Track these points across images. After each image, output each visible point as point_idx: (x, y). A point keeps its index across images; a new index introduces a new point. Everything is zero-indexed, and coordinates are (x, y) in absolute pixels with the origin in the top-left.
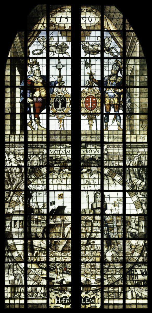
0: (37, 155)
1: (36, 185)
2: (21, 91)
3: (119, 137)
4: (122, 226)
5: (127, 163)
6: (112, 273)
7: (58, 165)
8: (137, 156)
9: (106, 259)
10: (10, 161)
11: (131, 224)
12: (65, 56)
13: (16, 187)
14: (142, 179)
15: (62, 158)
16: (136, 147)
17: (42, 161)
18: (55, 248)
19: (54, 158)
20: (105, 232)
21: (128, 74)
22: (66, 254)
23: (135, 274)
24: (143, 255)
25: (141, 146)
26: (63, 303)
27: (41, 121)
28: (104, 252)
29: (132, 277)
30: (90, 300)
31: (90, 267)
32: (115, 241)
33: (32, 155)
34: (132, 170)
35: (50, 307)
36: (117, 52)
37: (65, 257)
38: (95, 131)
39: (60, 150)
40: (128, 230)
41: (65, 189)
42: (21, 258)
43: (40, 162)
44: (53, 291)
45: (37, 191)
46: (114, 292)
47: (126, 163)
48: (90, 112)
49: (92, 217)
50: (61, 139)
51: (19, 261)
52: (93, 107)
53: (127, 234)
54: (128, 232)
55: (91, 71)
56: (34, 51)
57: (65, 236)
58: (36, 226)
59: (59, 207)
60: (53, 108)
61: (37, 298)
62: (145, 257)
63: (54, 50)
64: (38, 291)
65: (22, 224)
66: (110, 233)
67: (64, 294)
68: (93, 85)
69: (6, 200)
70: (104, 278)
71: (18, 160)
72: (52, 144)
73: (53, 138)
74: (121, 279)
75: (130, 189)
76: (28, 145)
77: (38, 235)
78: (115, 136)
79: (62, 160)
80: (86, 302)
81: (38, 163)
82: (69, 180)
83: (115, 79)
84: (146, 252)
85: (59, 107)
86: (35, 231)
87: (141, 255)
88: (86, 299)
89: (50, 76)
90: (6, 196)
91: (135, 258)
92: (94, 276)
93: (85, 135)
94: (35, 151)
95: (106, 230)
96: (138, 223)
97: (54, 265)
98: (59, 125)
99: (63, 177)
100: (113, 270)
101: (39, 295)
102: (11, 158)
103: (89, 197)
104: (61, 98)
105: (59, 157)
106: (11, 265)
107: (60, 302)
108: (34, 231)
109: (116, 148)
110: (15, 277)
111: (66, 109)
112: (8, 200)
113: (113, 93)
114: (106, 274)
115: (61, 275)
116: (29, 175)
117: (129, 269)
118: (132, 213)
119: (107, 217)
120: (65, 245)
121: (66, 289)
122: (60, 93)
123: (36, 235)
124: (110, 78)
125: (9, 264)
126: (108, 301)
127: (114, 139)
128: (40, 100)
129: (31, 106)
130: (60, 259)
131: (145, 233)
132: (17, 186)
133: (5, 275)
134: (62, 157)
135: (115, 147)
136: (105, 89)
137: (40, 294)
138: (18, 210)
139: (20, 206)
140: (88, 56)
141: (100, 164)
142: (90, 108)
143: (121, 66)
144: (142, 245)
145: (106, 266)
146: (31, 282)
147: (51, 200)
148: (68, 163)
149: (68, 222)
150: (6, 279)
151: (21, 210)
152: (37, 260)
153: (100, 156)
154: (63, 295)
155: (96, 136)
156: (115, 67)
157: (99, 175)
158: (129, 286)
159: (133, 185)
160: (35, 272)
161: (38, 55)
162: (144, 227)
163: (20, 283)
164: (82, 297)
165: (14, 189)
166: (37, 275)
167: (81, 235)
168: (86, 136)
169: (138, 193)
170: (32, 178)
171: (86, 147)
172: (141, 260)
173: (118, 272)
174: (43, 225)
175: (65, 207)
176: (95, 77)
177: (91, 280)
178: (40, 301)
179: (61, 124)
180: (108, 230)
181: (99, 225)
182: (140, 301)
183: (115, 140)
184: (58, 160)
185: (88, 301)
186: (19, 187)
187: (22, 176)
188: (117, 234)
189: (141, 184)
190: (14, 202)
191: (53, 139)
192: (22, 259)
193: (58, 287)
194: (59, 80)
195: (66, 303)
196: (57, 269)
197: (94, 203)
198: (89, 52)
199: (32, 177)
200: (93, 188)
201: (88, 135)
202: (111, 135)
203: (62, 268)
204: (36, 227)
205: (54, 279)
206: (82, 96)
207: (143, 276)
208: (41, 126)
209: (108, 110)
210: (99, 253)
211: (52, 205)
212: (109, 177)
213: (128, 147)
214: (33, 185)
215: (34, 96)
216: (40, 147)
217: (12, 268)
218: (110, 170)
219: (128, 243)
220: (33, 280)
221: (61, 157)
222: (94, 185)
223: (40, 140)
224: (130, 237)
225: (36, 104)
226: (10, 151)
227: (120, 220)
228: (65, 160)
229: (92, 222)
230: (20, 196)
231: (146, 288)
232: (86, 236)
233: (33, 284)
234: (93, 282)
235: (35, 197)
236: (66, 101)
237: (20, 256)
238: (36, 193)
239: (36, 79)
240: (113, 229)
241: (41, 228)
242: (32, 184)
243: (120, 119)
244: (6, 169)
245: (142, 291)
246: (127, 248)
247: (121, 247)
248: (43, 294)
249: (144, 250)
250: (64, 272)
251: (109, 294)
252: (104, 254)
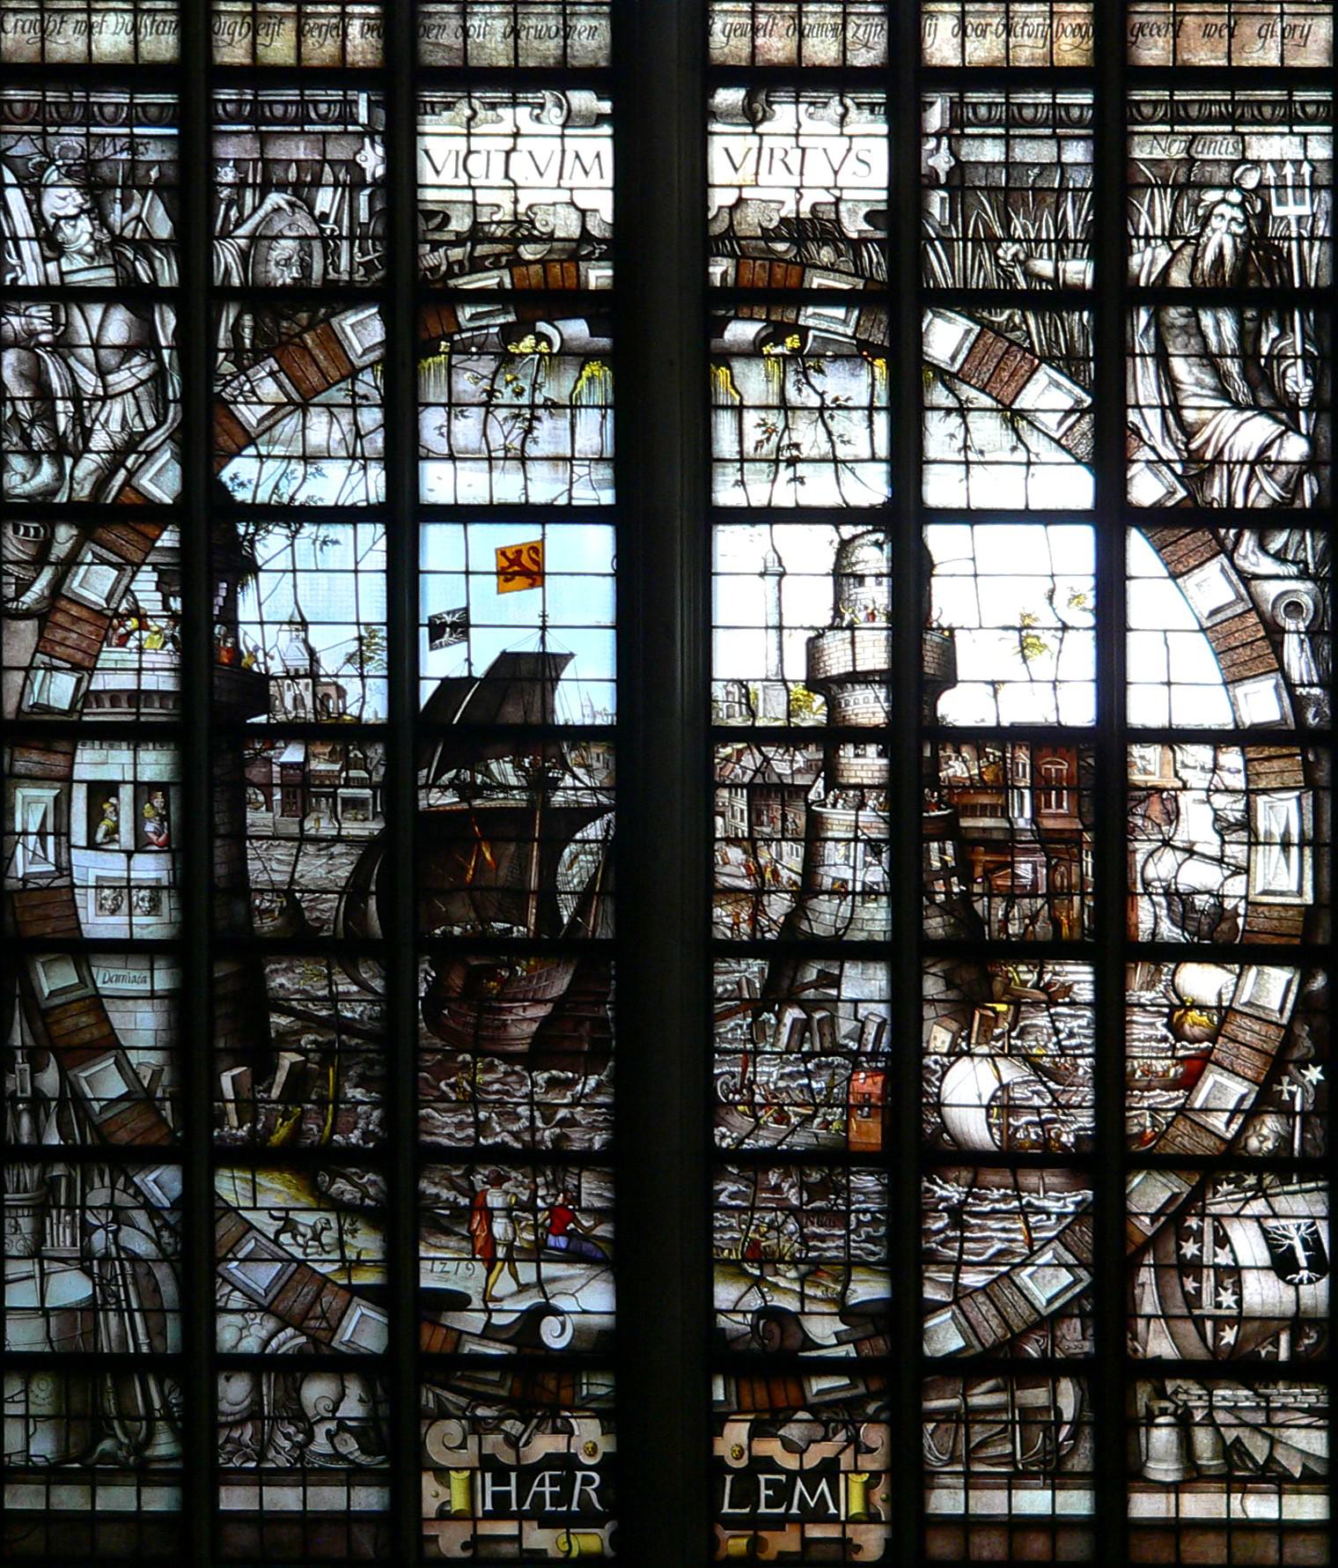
0: (302, 192)
1: (298, 468)
3: (1066, 22)
4: (1087, 837)
5: (1146, 261)
6: (1000, 1253)
7: (500, 284)
8: (1235, 196)
9: (944, 1127)
10: (51, 242)
11: (1173, 816)
13: (102, 483)
14: (1283, 409)
15: (532, 222)
16: (1221, 120)
17: (345, 245)
18: (477, 1026)
19: (460, 223)
20: (939, 886)
22: (570, 1084)
23: (1216, 1267)
24: (1286, 1097)
25: (1267, 111)
26: (548, 1508)
28: (929, 1061)
29: (1190, 1285)
30: (800, 1485)
31: (795, 1202)
32: (1022, 968)
33: (254, 186)
34: (1184, 328)
35: (430, 1550)
37: (562, 1113)
39: (514, 149)
40: (1151, 873)
41: (562, 501)
42: (158, 1112)
43: (331, 254)
44: (451, 1408)
45: (294, 515)
46: (1013, 1422)
47: (1135, 260)
49: (813, 753)
51: (138, 1141)
53: (1143, 903)
54: (1146, 884)
57: (566, 920)
58: (295, 830)
59: (507, 660)
61: (305, 1472)
62: (1302, 1112)
64: (310, 1412)
65: (164, 818)
66: (982, 896)
67: (555, 1431)
69: (16, 599)
70: (930, 1293)
71: (128, 233)
72: (437, 96)
73: (450, 38)
74: (1081, 1308)
75: (1171, 493)
76: (223, 95)
77: (312, 909)
78: (1028, 16)
79: (532, 239)
80: (762, 1510)
81: (310, 266)
82: (595, 414)
84: (1314, 1074)
86: (286, 878)
87: (1266, 1100)
88: (762, 1478)
90: (17, 563)
91: (1218, 1122)
92: (836, 1281)
94: (279, 151)
95: (942, 860)
96: (1241, 805)
97: (465, 1184)
99: (535, 387)
100: (1004, 1230)
101: (321, 1444)
102: (58, 218)
103: (785, 579)
105: (508, 208)
106: (63, 1182)
107: (520, 1503)
108: (276, 877)
109: (1033, 123)
110: (101, 1283)
112: (29, 598)
114: (944, 1263)
115: (527, 1272)
116: (227, 368)
117: (1154, 1217)
118: (1186, 719)
119: (958, 752)
120: (559, 1002)
121: (565, 1394)
123: (293, 910)
125: (43, 1173)
126: (962, 1494)
127: (1012, 40)
130: (515, 1128)
131: (1308, 898)
132: (113, 473)
133: (13, 1269)
134: (530, 207)
135: (1028, 113)
137: (330, 1436)
138: (126, 682)
139: (141, 650)
141: (881, 275)
144: (1281, 1010)
145: (940, 1192)
146: (247, 1327)
147: (437, 598)
148: (583, 265)
149: (588, 800)
150: (20, 1295)
151: (149, 682)
152: (297, 1132)
153: (883, 207)
154: (545, 1444)
157: (874, 379)
158: (1160, 1369)
159: (1193, 458)
160: (285, 1238)
162: (1301, 846)
163: (142, 1338)
164: (722, 1457)
165: (87, 491)
166: (302, 1263)
167: (717, 911)
169: (1239, 537)
170: (261, 403)
171: (752, 116)
172: (1269, 1145)
173: (1056, 1244)
174: (352, 828)
175: (564, 659)
177: (803, 1313)
178: (330, 1498)
180: (964, 869)
181: (872, 820)
182: (1260, 1507)
183: (1028, 52)
184: (493, 240)
185: (782, 1493)
186: (134, 482)
187: (158, 378)
188: (1040, 902)
189: (1273, 454)
190: (85, 614)
191: (450, 48)
192: (165, 1120)
193: (494, 1376)
195: (575, 1508)
196: (489, 1215)
197: (831, 627)
199: (253, 391)
200: (820, 489)
203: (531, 1207)
204: (288, 839)
205: (459, 1301)
207: (1290, 1282)
210: (879, 1079)
211: (441, 646)
212: (973, 393)
213: (1147, 121)
214: (270, 465)
216: (324, 120)
217: (70, 1208)
218: (977, 329)
219: (1150, 986)
220: (266, 1310)
221: (521, 208)
222: (835, 460)
223: (321, 50)
224: (1169, 931)
226: (45, 152)
227: (1070, 777)
228: (559, 234)
229: (812, 796)
230: (143, 563)
231: (1311, 1396)
232: (753, 920)
233: (266, 1343)
234: (823, 1329)
235: (284, 571)
237: (140, 1097)
238: (294, 537)
240: (1012, 865)
241: (338, 849)
242: (259, 456)
244: (18, 314)
245: (1279, 1418)
246: (1145, 1030)
247: (1079, 1024)
248: (357, 1434)
249: (1296, 1054)
250: (552, 1240)
251: (976, 1440)
252: (929, 1082)
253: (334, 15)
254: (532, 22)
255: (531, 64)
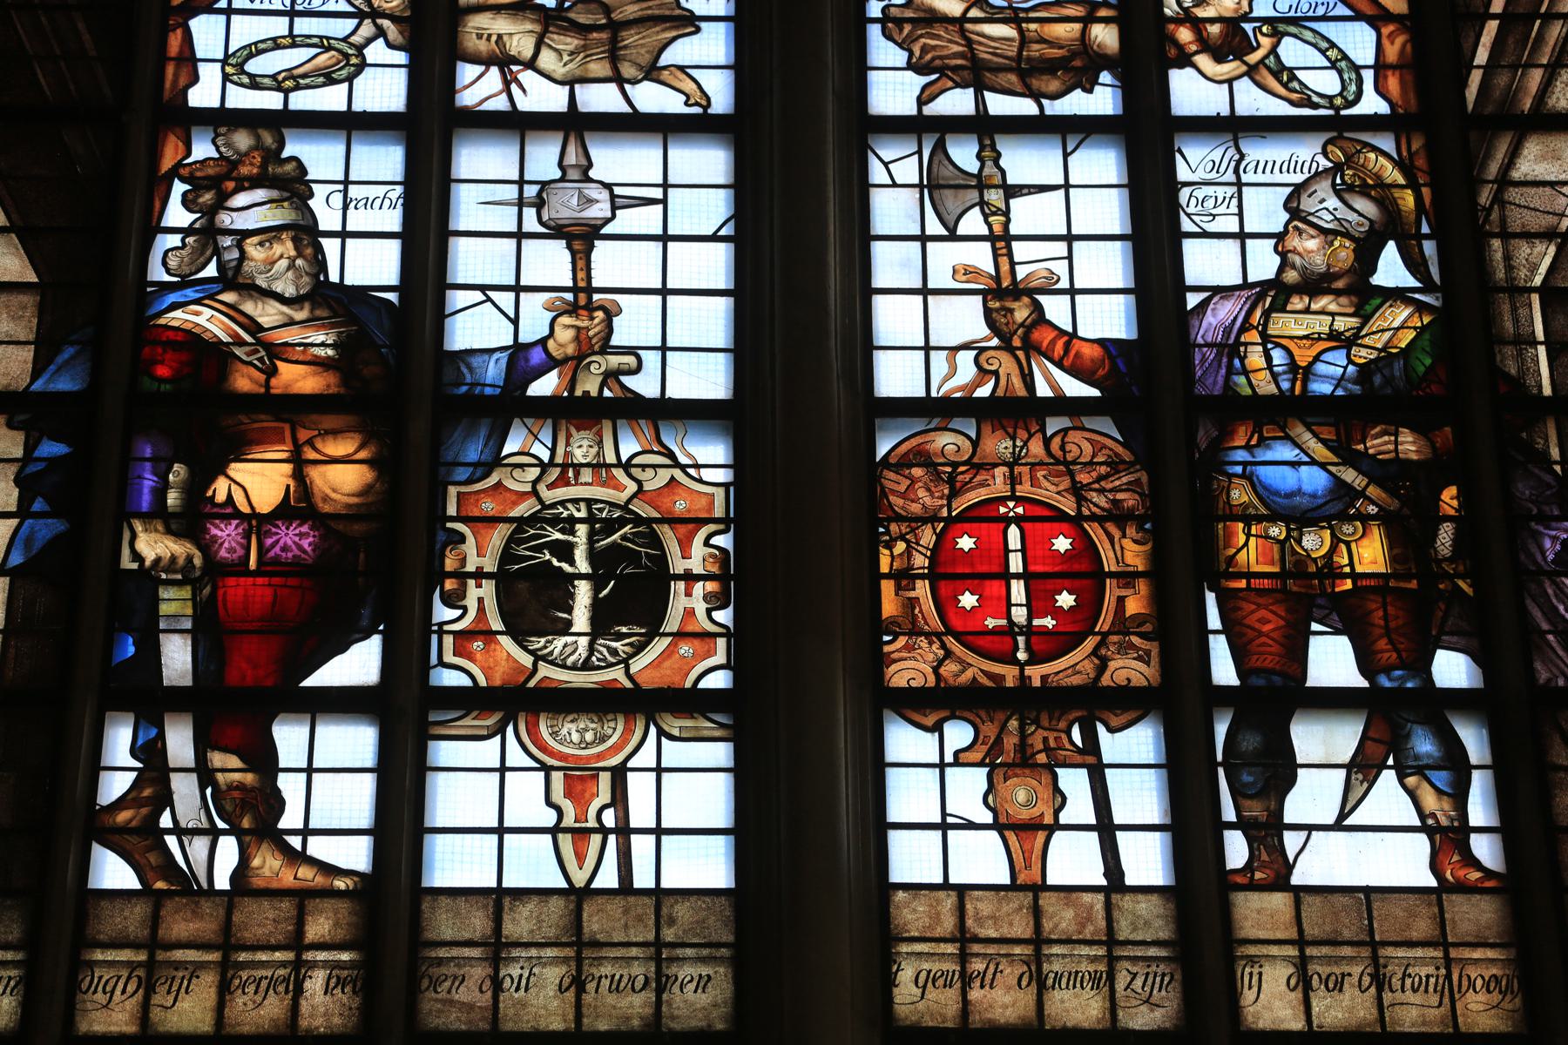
2: (29, 448)
12: (652, 98)
21: (1523, 273)
27: (290, 786)
36: (1340, 62)
38: (1087, 898)
48: (1010, 683)
50: (588, 998)
52: (1049, 622)
55: (1010, 255)
56: (255, 50)
60: (489, 635)
63: (522, 45)
68: (1043, 390)
73: (471, 991)
83: (1341, 324)
85: (565, 628)
89: (458, 299)
93: (950, 949)
98: (554, 831)
104: (600, 526)
111: (659, 645)
113: (1323, 466)
122: (587, 475)
124: (1267, 315)
127: (1387, 997)
128: (295, 539)
129: (165, 609)
136: (1203, 437)
140: (957, 102)
142: (1011, 630)
143: (1408, 200)
155: (1112, 960)
156: (1333, 202)
161: (297, 88)
168: (963, 958)
176: (1056, 309)
179: (592, 823)
191: (470, 1007)
194: (564, 335)
198: (978, 75)
201: (991, 950)
202: (1347, 951)
206: (896, 501)
208: (287, 851)
209: (1269, 656)
215: (221, 497)
225: (235, 590)
236: (662, 560)
239: (253, 327)
243: (1456, 763)
253: (283, 964)
254: (606, 970)
255: (603, 1026)
